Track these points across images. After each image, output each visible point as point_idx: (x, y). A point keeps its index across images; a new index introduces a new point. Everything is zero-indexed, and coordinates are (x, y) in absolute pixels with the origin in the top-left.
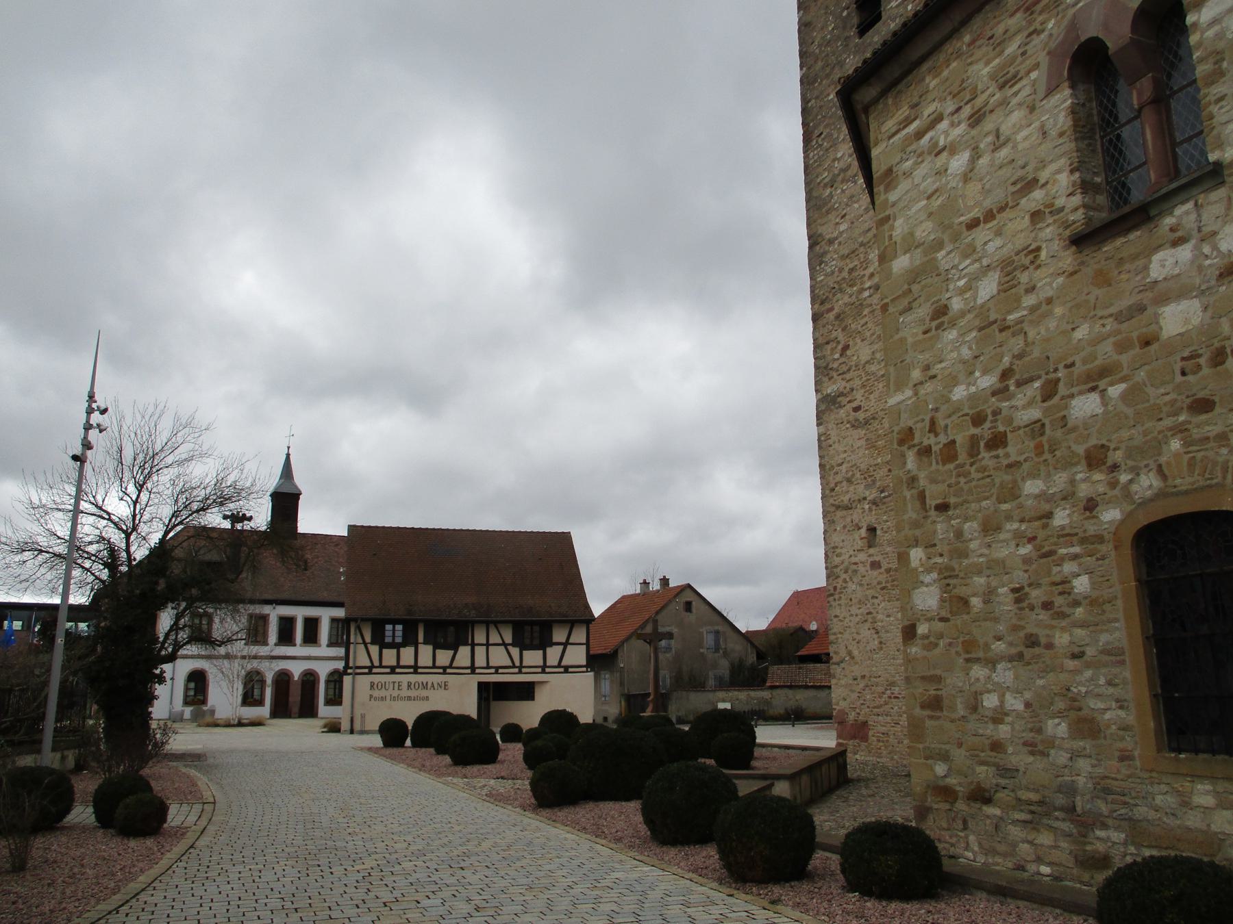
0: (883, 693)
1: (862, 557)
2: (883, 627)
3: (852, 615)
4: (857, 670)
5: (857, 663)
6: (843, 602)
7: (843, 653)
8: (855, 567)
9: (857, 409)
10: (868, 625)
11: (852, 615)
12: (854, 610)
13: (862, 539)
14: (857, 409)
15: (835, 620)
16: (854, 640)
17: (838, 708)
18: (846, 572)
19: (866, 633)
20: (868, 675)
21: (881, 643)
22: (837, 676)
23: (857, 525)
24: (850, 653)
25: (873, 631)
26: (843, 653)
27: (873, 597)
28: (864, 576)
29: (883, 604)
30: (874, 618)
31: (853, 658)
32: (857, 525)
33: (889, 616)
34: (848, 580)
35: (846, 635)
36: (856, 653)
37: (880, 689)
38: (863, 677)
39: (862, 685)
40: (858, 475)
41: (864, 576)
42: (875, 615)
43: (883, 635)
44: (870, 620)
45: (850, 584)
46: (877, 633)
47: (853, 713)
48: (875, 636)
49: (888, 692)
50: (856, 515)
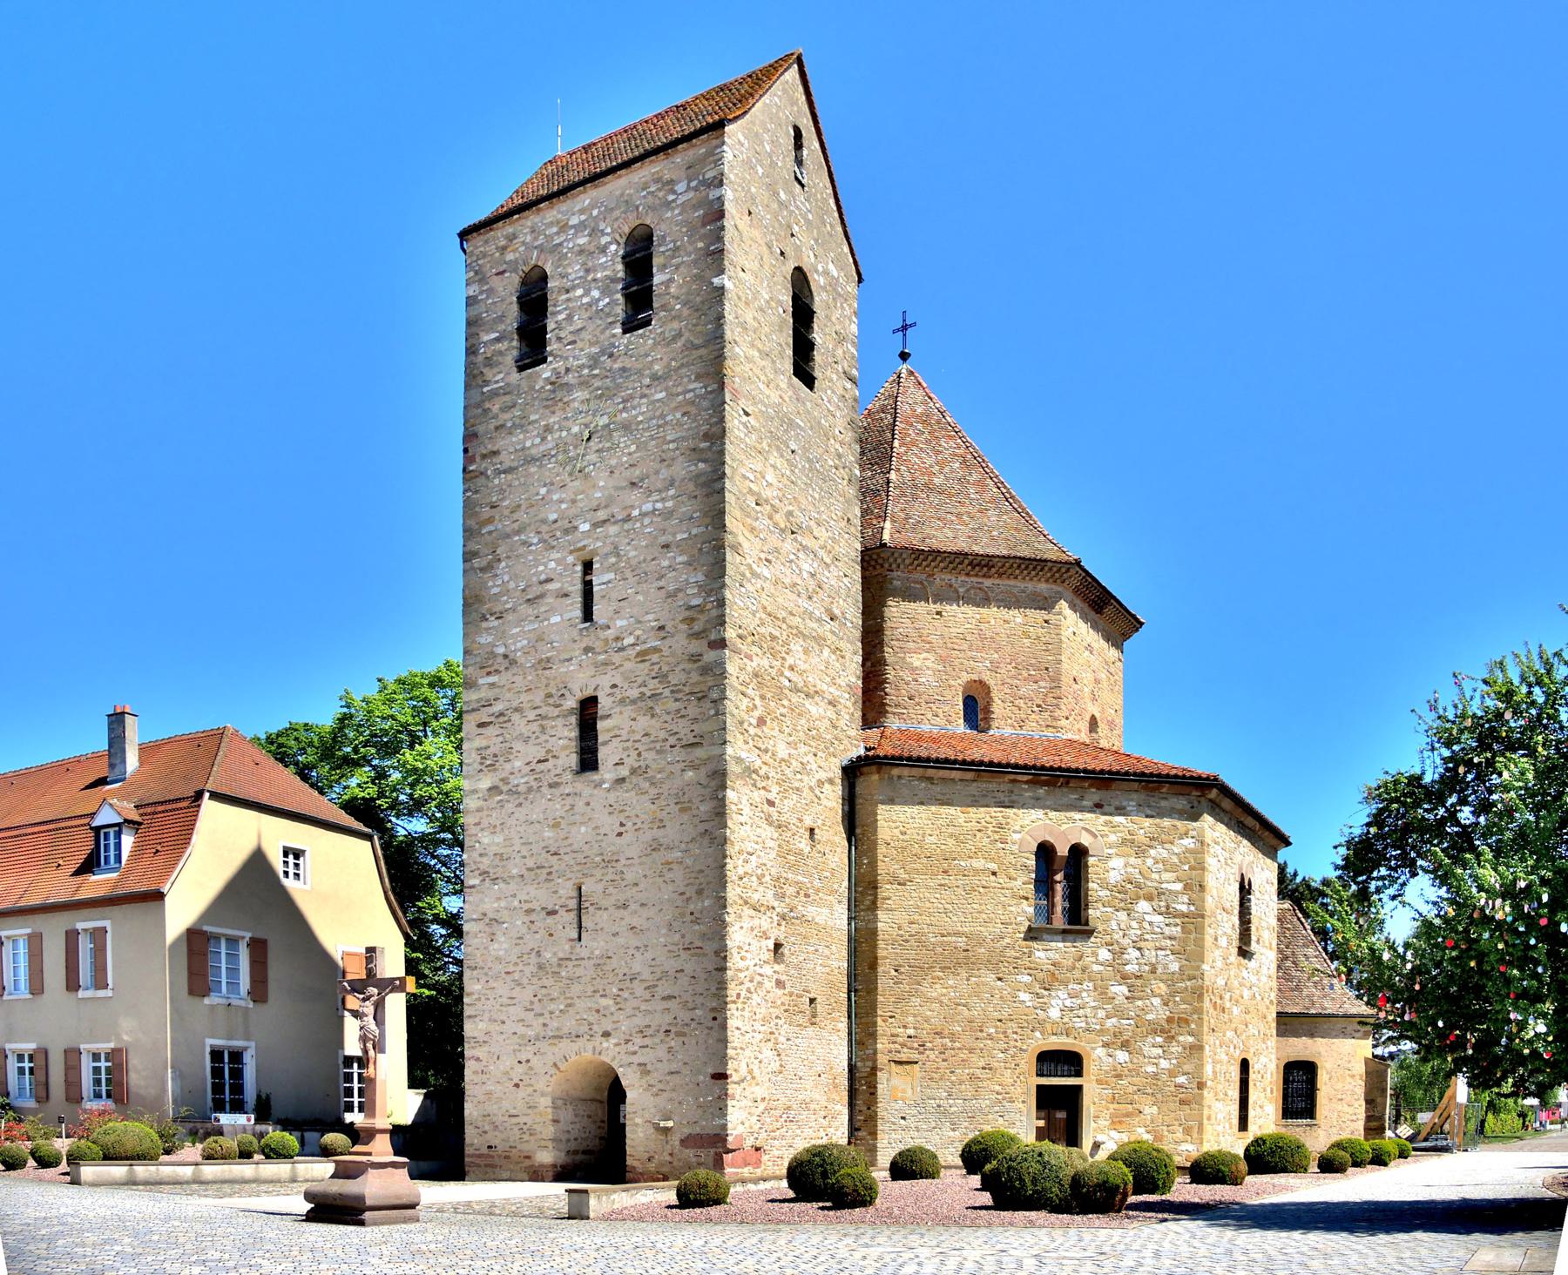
0: (781, 1117)
1: (767, 970)
2: (784, 1049)
3: (754, 1031)
4: (759, 1092)
5: (758, 1084)
6: (746, 1014)
7: (743, 1070)
8: (758, 978)
9: (771, 803)
10: (770, 1045)
11: (754, 1031)
12: (757, 1026)
13: (768, 950)
14: (771, 803)
15: (737, 1032)
16: (756, 1058)
17: (735, 1133)
18: (751, 981)
19: (768, 1054)
20: (768, 1098)
21: (781, 1066)
22: (737, 1097)
23: (764, 933)
24: (750, 1072)
25: (776, 1053)
26: (743, 1070)
27: (777, 1017)
28: (769, 992)
29: (785, 1026)
30: (776, 1039)
31: (753, 1078)
32: (764, 933)
33: (788, 1040)
34: (752, 990)
35: (748, 1053)
36: (756, 1072)
37: (778, 1113)
38: (763, 1099)
39: (762, 1106)
40: (768, 878)
41: (769, 992)
42: (777, 1035)
43: (782, 1057)
44: (773, 1041)
45: (755, 996)
46: (779, 1055)
47: (752, 1138)
48: (777, 1058)
49: (785, 1116)
50: (764, 922)
